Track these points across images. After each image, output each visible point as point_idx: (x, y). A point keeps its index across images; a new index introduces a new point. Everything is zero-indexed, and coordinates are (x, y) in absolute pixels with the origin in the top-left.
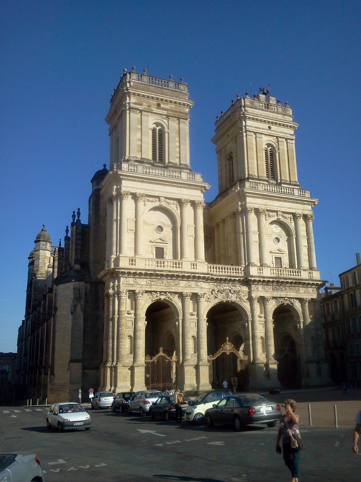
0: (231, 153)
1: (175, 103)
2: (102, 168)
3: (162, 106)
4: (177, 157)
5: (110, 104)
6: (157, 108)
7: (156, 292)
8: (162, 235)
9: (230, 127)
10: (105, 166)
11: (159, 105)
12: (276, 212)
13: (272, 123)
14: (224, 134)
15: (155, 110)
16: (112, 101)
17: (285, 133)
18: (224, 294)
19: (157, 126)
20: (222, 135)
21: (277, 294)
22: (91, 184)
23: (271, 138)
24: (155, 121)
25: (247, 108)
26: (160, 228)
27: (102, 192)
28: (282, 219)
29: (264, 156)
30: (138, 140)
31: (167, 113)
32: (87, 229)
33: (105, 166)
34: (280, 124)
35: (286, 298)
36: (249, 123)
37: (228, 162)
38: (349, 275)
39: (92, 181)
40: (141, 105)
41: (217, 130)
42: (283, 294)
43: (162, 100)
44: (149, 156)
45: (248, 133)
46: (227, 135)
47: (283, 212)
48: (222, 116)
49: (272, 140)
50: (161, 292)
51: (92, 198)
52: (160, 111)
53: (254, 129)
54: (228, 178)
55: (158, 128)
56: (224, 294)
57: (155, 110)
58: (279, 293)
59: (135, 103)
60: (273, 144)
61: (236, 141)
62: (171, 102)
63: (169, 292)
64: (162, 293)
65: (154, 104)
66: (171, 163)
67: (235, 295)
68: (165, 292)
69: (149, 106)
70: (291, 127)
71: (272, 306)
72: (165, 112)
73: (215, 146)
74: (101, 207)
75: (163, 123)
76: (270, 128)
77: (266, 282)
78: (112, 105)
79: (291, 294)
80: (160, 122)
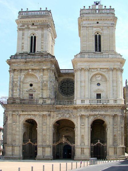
1: (41, 21)
3: (35, 24)
4: (41, 48)
6: (32, 26)
8: (32, 88)
11: (33, 24)
12: (97, 68)
13: (99, 19)
15: (30, 27)
17: (108, 24)
18: (62, 115)
21: (92, 113)
23: (99, 29)
24: (31, 33)
25: (83, 15)
26: (31, 85)
28: (101, 72)
29: (94, 39)
30: (23, 43)
31: (37, 27)
34: (104, 19)
35: (98, 115)
36: (84, 22)
40: (24, 26)
42: (97, 113)
43: (34, 21)
44: (28, 51)
45: (83, 28)
47: (100, 68)
49: (99, 29)
52: (33, 27)
53: (87, 25)
55: (33, 36)
57: (30, 27)
58: (94, 113)
59: (21, 26)
60: (100, 31)
62: (39, 21)
63: (32, 115)
64: (29, 115)
65: (31, 24)
67: (68, 115)
69: (28, 26)
70: (111, 19)
71: (92, 119)
72: (36, 27)
75: (35, 33)
76: (98, 23)
77: (86, 108)
79: (102, 113)
80: (34, 32)
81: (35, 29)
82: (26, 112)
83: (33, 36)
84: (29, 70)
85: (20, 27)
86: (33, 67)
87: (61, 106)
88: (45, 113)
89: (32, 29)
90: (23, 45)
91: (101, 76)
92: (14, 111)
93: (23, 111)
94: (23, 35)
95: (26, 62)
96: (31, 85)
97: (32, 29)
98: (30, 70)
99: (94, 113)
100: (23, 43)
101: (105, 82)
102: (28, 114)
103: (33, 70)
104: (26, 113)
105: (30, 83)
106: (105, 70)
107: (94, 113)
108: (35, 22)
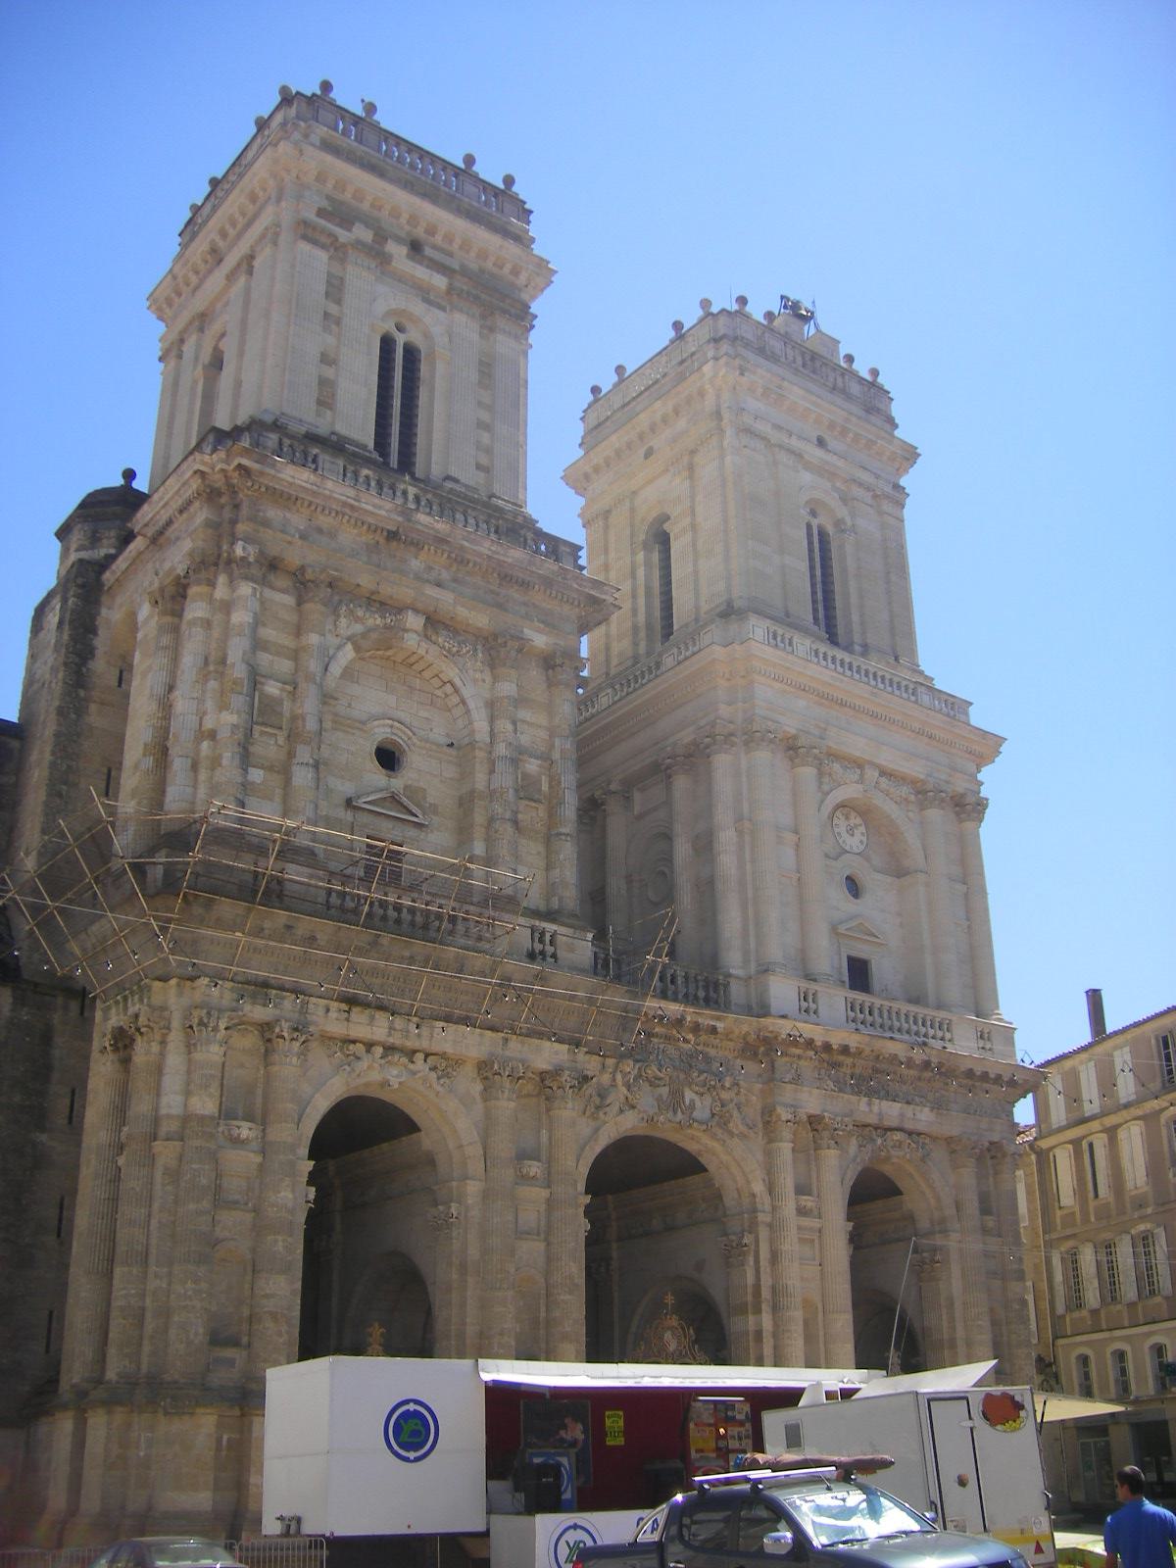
0: (665, 518)
2: (118, 481)
5: (173, 245)
7: (369, 1046)
8: (397, 783)
9: (665, 420)
10: (130, 475)
14: (629, 446)
16: (191, 228)
19: (400, 328)
20: (618, 453)
22: (57, 545)
27: (108, 577)
32: (15, 744)
33: (130, 475)
35: (898, 1136)
37: (640, 556)
38: (1082, 1068)
39: (63, 533)
41: (588, 442)
42: (891, 1111)
46: (642, 451)
48: (615, 386)
50: (389, 1049)
51: (57, 604)
52: (421, 273)
54: (641, 618)
56: (664, 1091)
61: (691, 468)
66: (456, 481)
68: (411, 1054)
72: (440, 282)
73: (581, 501)
74: (101, 643)
78: (184, 246)
81: (425, 293)
82: (382, 1019)
83: (401, 340)
84: (400, 610)
85: (312, 216)
86: (445, 600)
87: (673, 1008)
88: (548, 1054)
89: (401, 279)
90: (329, 372)
91: (862, 829)
92: (265, 984)
93: (351, 1001)
94: (335, 289)
95: (392, 536)
96: (388, 758)
97: (401, 279)
98: (414, 621)
99: (868, 1109)
100: (326, 359)
101: (889, 879)
102: (396, 1040)
103: (434, 622)
104: (377, 1028)
105: (381, 732)
106: (905, 791)
107: (868, 1109)
108: (438, 239)
